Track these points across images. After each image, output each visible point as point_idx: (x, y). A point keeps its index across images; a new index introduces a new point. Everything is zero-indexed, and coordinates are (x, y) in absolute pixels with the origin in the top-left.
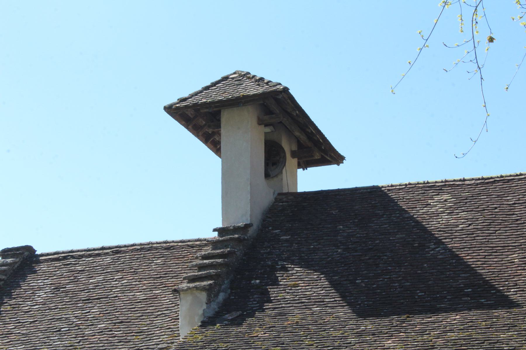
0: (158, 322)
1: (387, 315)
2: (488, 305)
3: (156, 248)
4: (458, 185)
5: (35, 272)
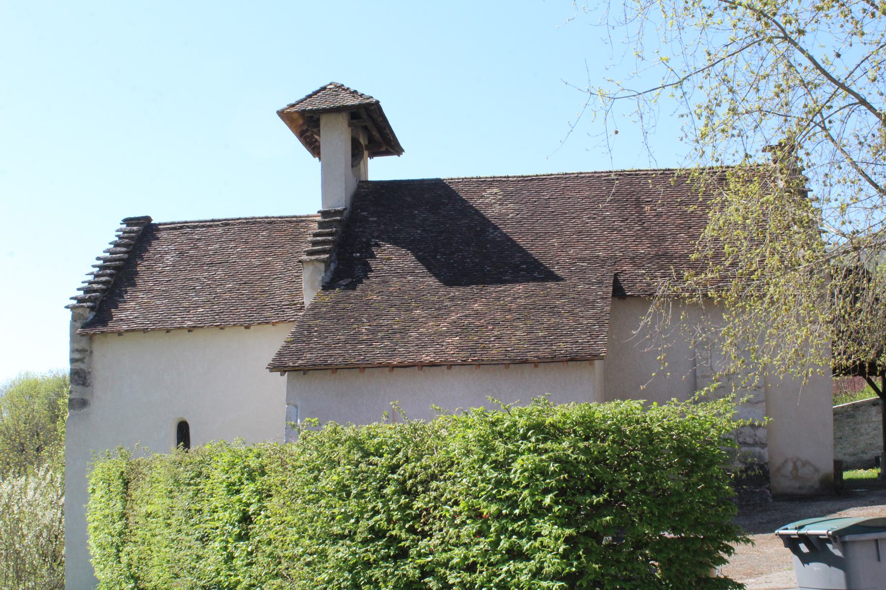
0: (276, 283)
1: (467, 284)
2: (539, 278)
3: (260, 222)
4: (504, 181)
5: (158, 239)
